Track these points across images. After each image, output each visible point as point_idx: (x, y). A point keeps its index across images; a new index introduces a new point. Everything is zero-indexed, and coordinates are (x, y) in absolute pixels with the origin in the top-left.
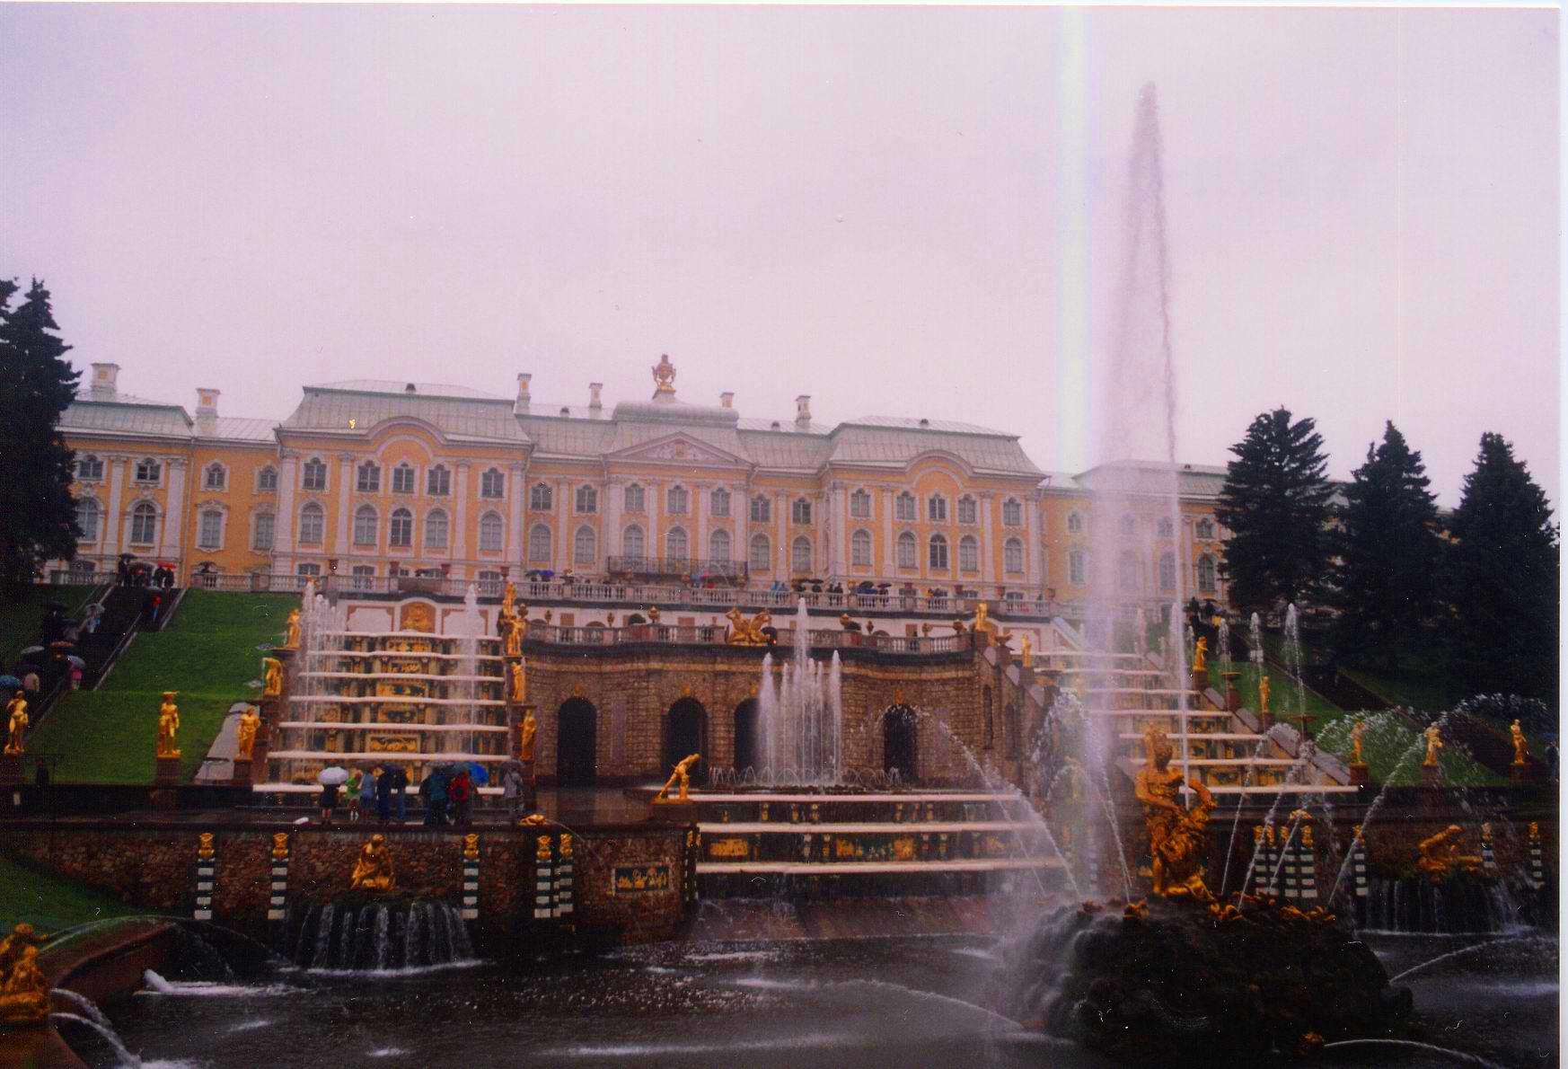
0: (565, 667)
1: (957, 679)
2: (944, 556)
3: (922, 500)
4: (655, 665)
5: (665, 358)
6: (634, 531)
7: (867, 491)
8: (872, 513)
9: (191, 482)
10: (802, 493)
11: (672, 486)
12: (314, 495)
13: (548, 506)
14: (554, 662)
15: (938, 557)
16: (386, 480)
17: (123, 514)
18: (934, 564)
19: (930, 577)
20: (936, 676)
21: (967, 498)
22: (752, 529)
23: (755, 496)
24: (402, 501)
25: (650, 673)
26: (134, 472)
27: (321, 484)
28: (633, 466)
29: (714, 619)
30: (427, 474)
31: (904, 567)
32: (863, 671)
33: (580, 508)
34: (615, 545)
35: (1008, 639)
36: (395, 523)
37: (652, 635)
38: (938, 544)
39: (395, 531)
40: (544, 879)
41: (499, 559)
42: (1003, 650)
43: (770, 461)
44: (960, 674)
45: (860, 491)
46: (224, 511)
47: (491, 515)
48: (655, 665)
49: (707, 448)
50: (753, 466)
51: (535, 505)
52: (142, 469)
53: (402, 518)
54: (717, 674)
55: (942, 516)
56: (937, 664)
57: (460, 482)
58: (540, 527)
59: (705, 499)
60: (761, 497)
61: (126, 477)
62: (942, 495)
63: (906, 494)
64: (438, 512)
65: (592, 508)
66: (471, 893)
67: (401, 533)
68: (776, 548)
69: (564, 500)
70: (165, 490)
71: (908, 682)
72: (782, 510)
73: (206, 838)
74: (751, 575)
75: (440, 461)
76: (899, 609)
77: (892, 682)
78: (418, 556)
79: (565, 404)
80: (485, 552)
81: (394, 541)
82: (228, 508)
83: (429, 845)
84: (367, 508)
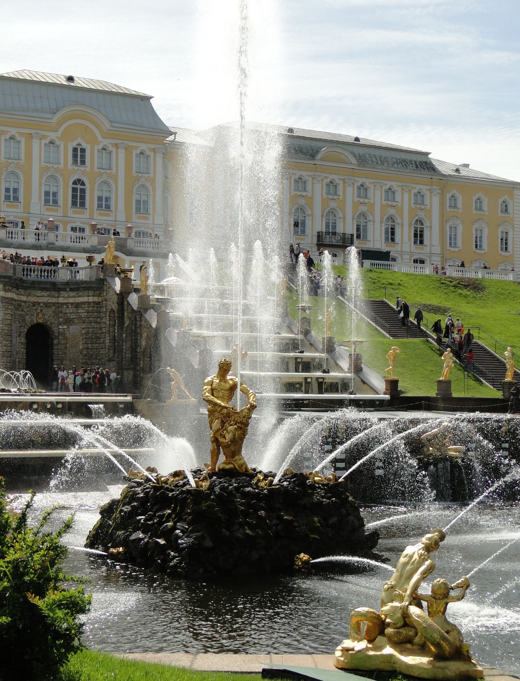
1: (89, 303)
2: (83, 197)
3: (66, 147)
7: (18, 138)
8: (23, 156)
15: (78, 198)
18: (74, 204)
20: (71, 300)
35: (131, 271)
38: (79, 187)
42: (126, 281)
44: (91, 299)
45: (12, 138)
55: (83, 162)
56: (72, 290)
62: (84, 145)
63: (52, 142)
71: (47, 305)
77: (34, 304)
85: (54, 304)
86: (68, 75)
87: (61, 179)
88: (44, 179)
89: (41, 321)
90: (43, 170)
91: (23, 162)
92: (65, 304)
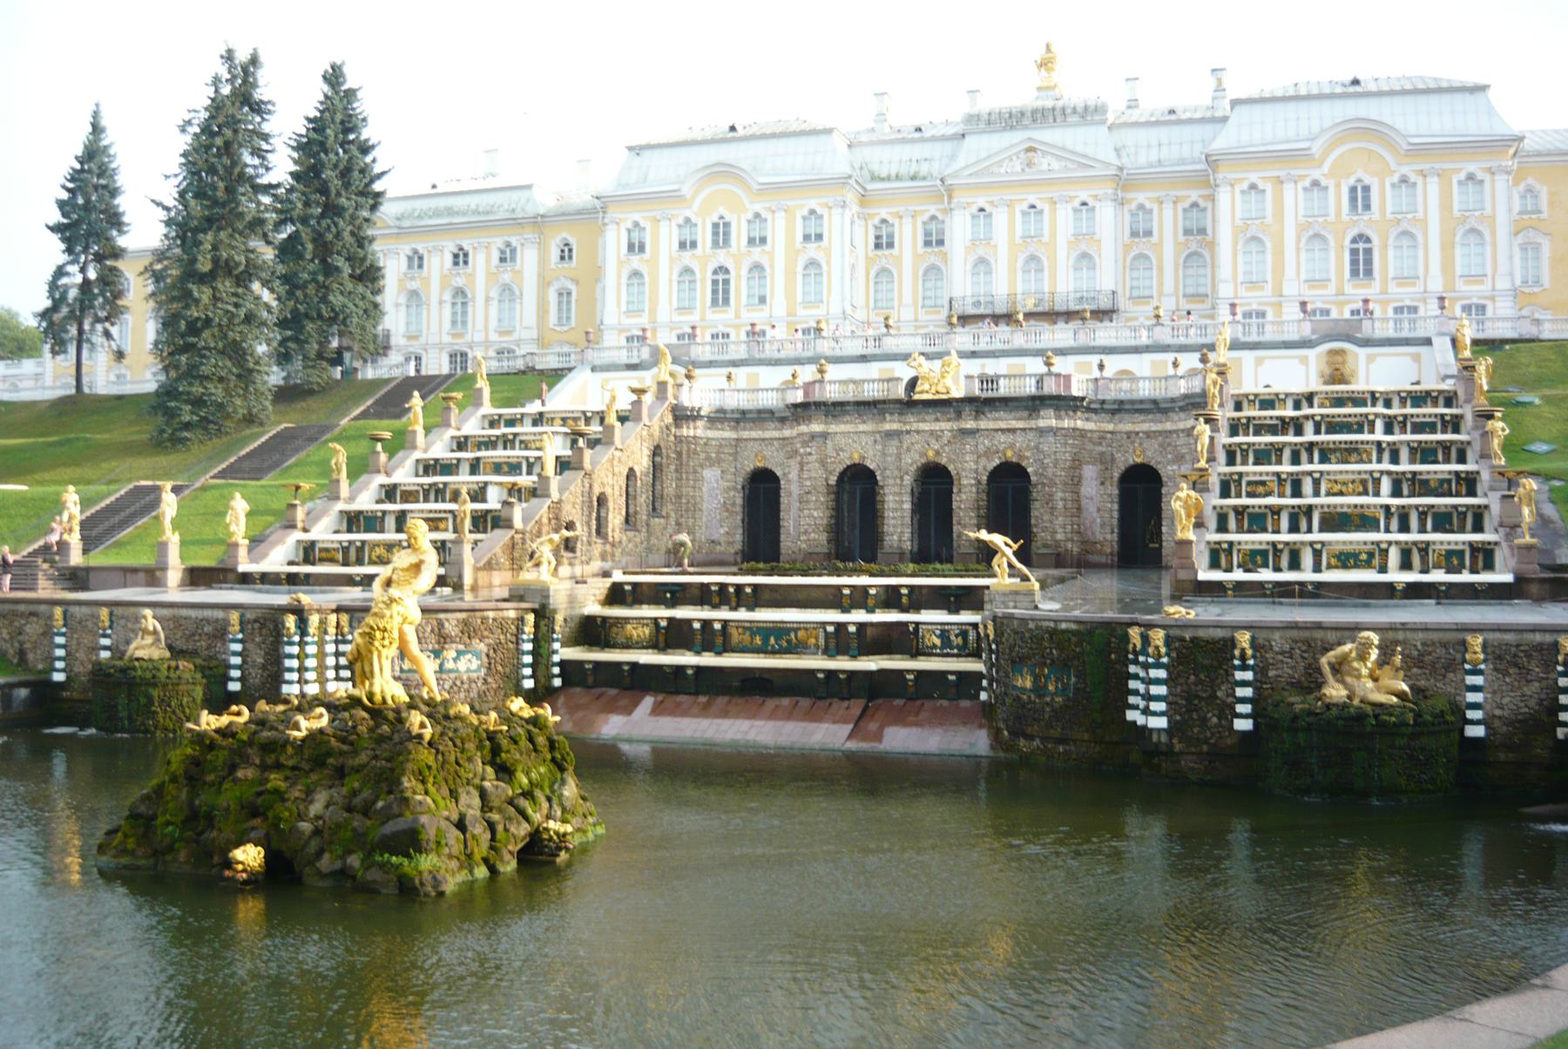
0: (746, 434)
2: (1369, 262)
3: (1338, 185)
4: (816, 427)
5: (1048, 49)
6: (982, 264)
8: (1269, 212)
9: (543, 260)
10: (1194, 195)
11: (1025, 206)
12: (636, 261)
13: (890, 245)
14: (735, 429)
15: (1361, 262)
16: (705, 237)
17: (488, 299)
18: (1355, 272)
19: (1349, 288)
20: (1181, 425)
21: (1404, 180)
22: (1127, 248)
23: (1133, 206)
24: (722, 257)
25: (813, 436)
26: (496, 255)
27: (642, 248)
28: (977, 186)
29: (983, 366)
30: (744, 225)
31: (1312, 282)
32: (1066, 423)
33: (927, 243)
34: (962, 287)
36: (715, 282)
37: (817, 396)
38: (1361, 246)
39: (715, 292)
40: (291, 656)
41: (820, 312)
43: (1153, 157)
45: (1253, 187)
46: (573, 287)
47: (813, 264)
48: (816, 427)
49: (1063, 154)
50: (1121, 169)
51: (878, 246)
52: (456, 256)
53: (720, 277)
54: (889, 435)
55: (1367, 207)
56: (1182, 409)
57: (777, 229)
58: (884, 271)
59: (1065, 214)
60: (1141, 207)
61: (488, 261)
62: (1367, 180)
63: (1315, 183)
64: (757, 267)
65: (941, 242)
66: (236, 667)
67: (721, 294)
68: (1161, 269)
69: (908, 236)
70: (520, 272)
71: (1148, 434)
72: (1168, 222)
73: (58, 612)
74: (1123, 303)
75: (758, 208)
76: (1391, 333)
77: (1129, 434)
78: (737, 316)
79: (917, 123)
80: (807, 304)
81: (715, 302)
82: (577, 282)
83: (208, 621)
84: (688, 270)
85: (1160, 433)
86: (1351, 78)
87: (1330, 237)
88: (1303, 241)
89: (1139, 460)
90: (1301, 228)
91: (1269, 219)
92: (1176, 431)
